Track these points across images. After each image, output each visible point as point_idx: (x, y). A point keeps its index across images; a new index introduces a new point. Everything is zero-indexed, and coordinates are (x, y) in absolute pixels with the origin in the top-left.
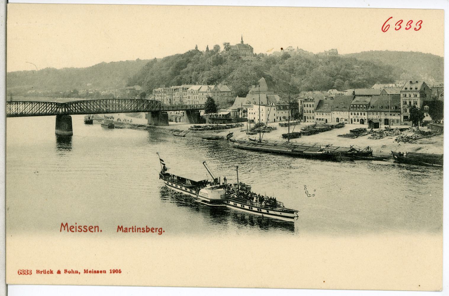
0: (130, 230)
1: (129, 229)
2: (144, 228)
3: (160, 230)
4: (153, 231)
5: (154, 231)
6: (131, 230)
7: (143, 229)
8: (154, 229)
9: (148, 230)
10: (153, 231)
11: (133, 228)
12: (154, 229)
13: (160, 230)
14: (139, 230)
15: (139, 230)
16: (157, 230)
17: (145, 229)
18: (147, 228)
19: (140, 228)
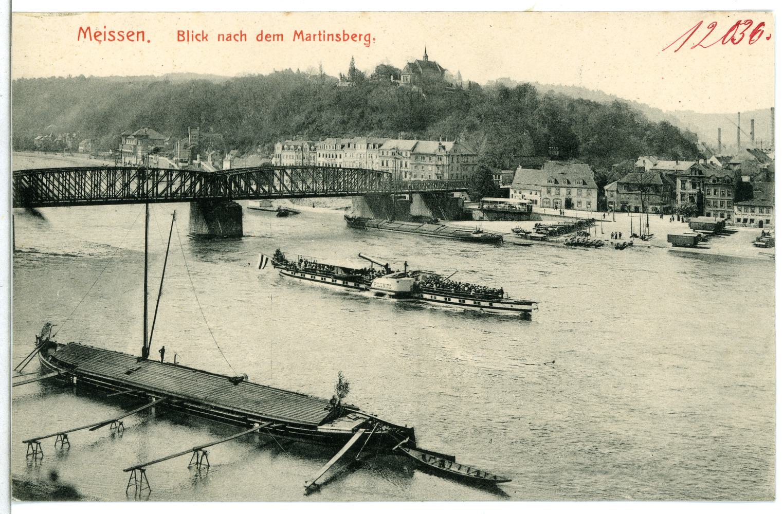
0: (316, 37)
1: (314, 35)
2: (339, 35)
3: (367, 39)
4: (355, 39)
5: (357, 39)
6: (317, 37)
7: (338, 35)
8: (356, 36)
9: (346, 37)
10: (355, 39)
11: (320, 34)
12: (356, 36)
13: (367, 39)
14: (331, 37)
15: (331, 37)
16: (362, 38)
17: (341, 37)
18: (344, 35)
19: (332, 35)
